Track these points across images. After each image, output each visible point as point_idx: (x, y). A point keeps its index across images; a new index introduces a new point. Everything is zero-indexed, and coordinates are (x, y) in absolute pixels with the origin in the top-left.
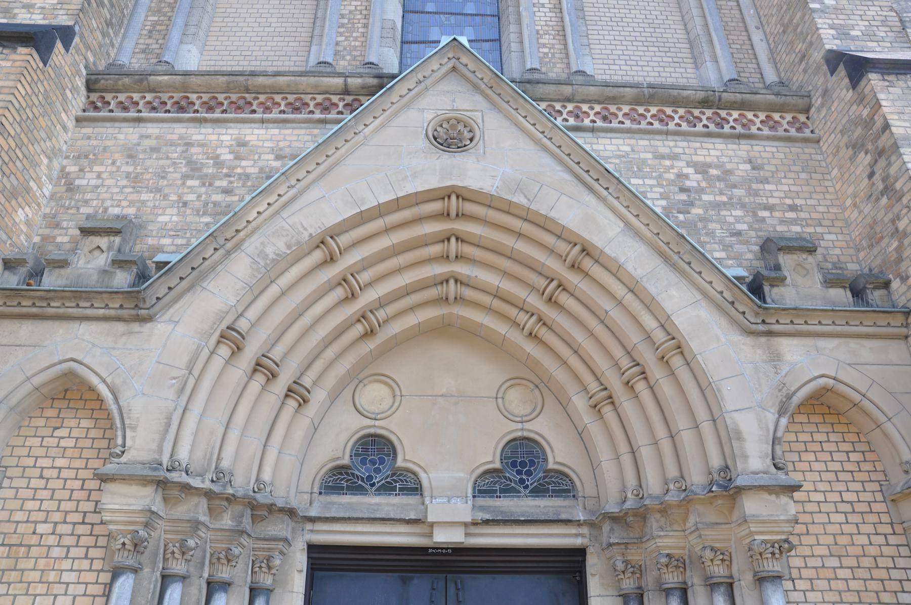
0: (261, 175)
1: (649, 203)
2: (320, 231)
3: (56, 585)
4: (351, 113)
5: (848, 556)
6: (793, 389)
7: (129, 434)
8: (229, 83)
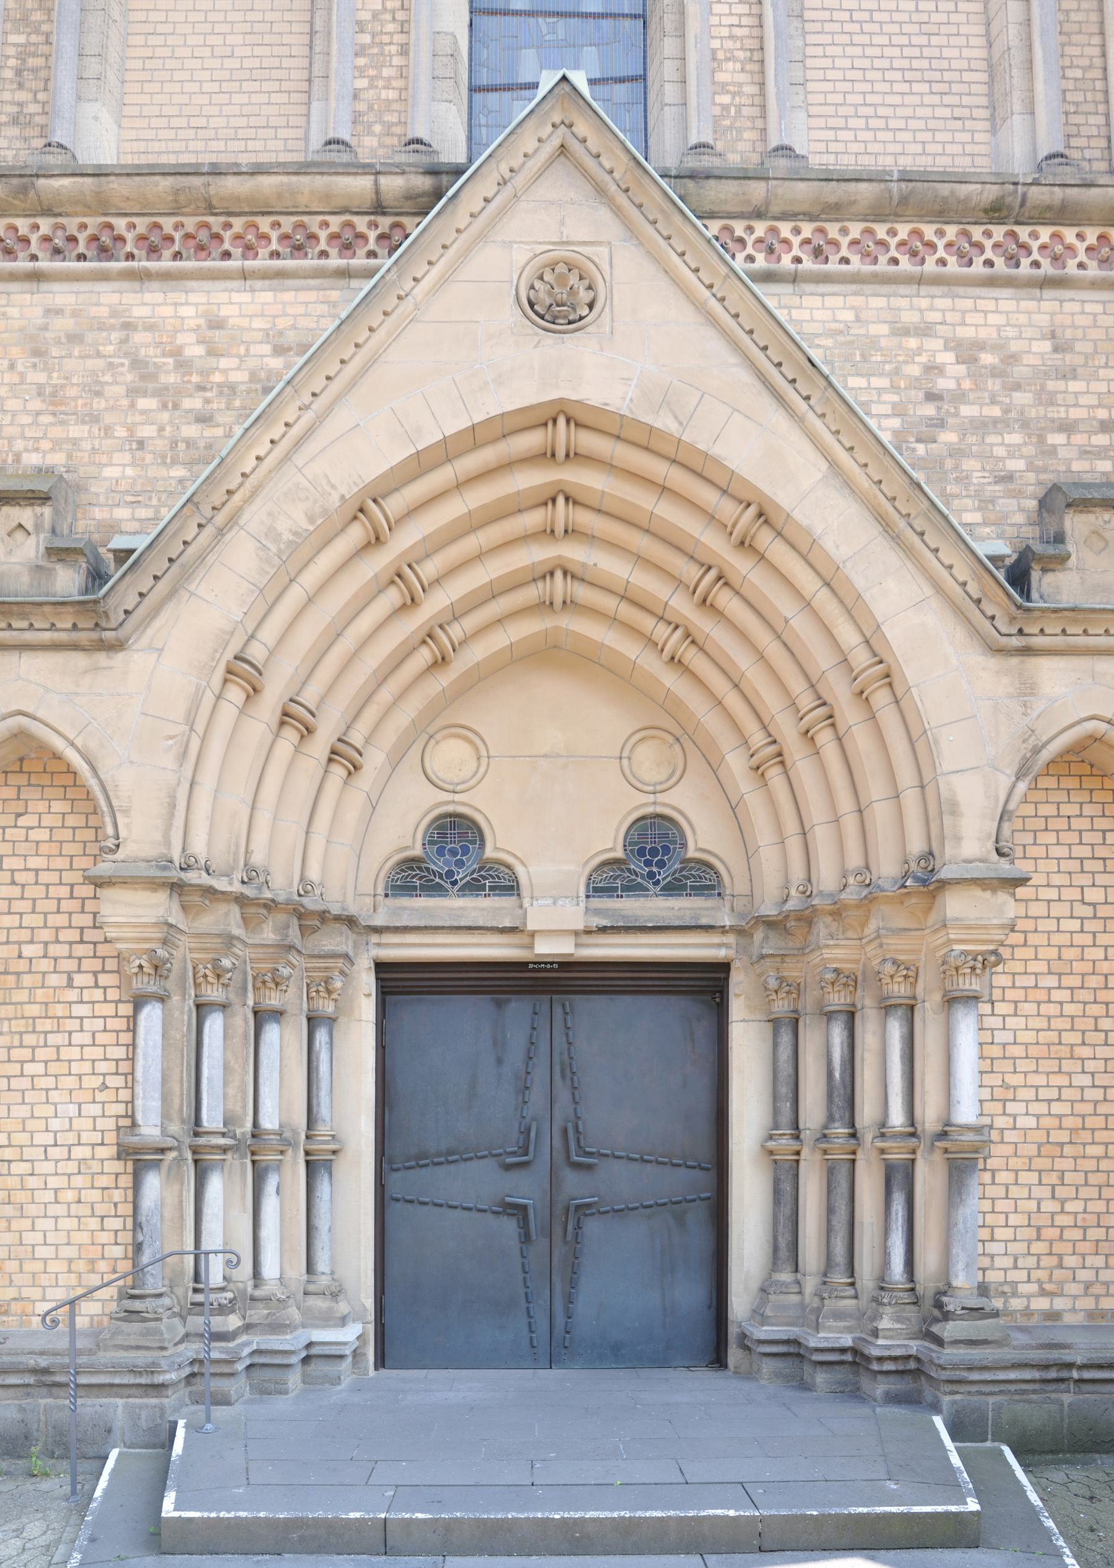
0: (254, 386)
1: (872, 423)
2: (356, 490)
3: (67, 1020)
4: (390, 254)
5: (1071, 974)
6: (1044, 738)
8: (177, 192)
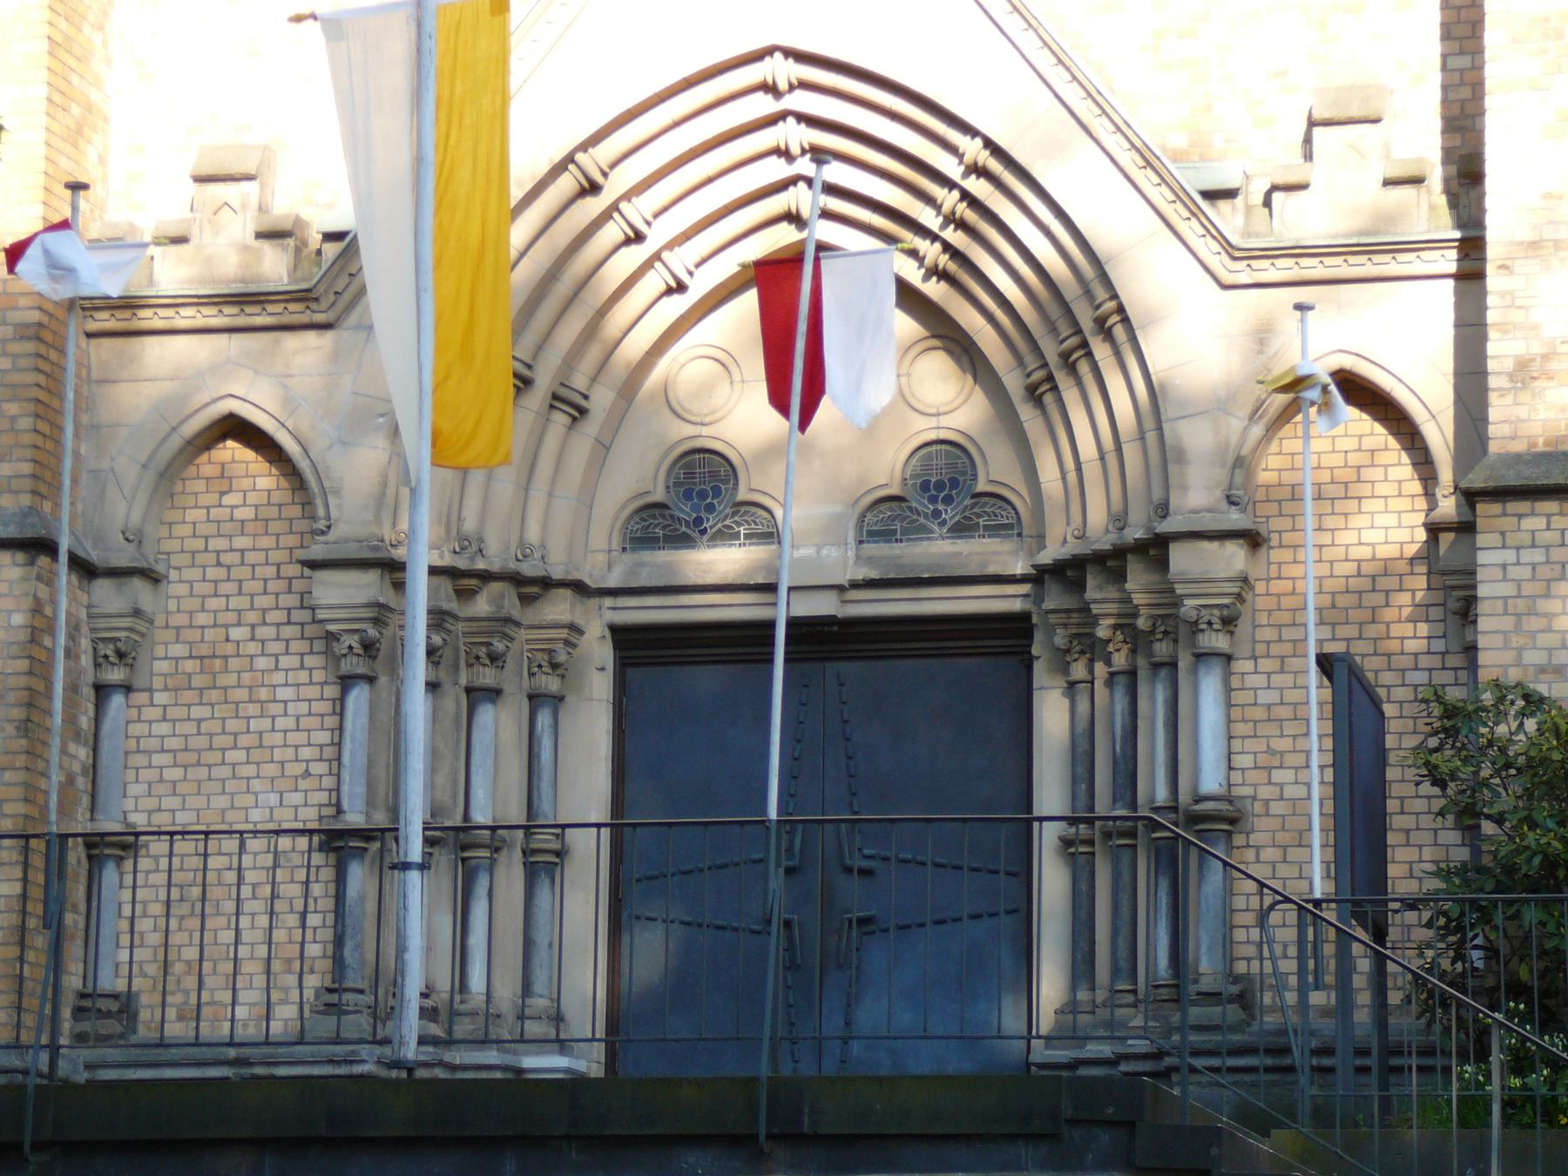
7: (332, 501)
